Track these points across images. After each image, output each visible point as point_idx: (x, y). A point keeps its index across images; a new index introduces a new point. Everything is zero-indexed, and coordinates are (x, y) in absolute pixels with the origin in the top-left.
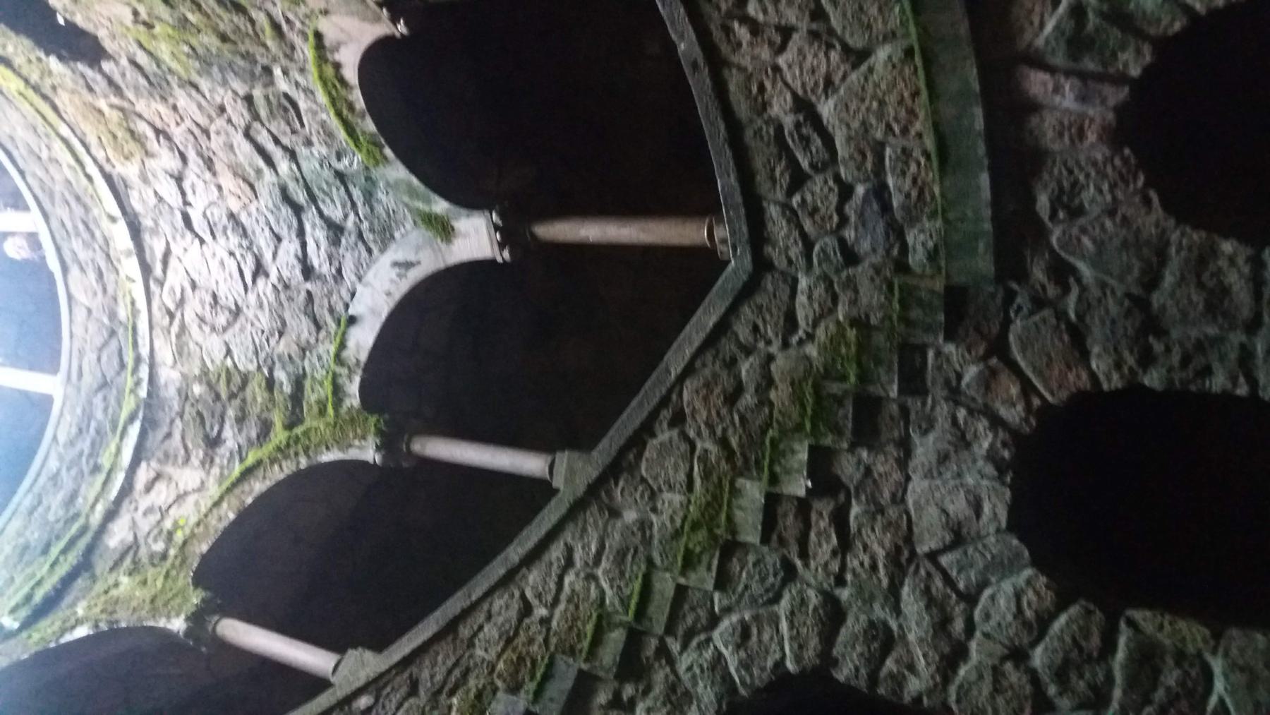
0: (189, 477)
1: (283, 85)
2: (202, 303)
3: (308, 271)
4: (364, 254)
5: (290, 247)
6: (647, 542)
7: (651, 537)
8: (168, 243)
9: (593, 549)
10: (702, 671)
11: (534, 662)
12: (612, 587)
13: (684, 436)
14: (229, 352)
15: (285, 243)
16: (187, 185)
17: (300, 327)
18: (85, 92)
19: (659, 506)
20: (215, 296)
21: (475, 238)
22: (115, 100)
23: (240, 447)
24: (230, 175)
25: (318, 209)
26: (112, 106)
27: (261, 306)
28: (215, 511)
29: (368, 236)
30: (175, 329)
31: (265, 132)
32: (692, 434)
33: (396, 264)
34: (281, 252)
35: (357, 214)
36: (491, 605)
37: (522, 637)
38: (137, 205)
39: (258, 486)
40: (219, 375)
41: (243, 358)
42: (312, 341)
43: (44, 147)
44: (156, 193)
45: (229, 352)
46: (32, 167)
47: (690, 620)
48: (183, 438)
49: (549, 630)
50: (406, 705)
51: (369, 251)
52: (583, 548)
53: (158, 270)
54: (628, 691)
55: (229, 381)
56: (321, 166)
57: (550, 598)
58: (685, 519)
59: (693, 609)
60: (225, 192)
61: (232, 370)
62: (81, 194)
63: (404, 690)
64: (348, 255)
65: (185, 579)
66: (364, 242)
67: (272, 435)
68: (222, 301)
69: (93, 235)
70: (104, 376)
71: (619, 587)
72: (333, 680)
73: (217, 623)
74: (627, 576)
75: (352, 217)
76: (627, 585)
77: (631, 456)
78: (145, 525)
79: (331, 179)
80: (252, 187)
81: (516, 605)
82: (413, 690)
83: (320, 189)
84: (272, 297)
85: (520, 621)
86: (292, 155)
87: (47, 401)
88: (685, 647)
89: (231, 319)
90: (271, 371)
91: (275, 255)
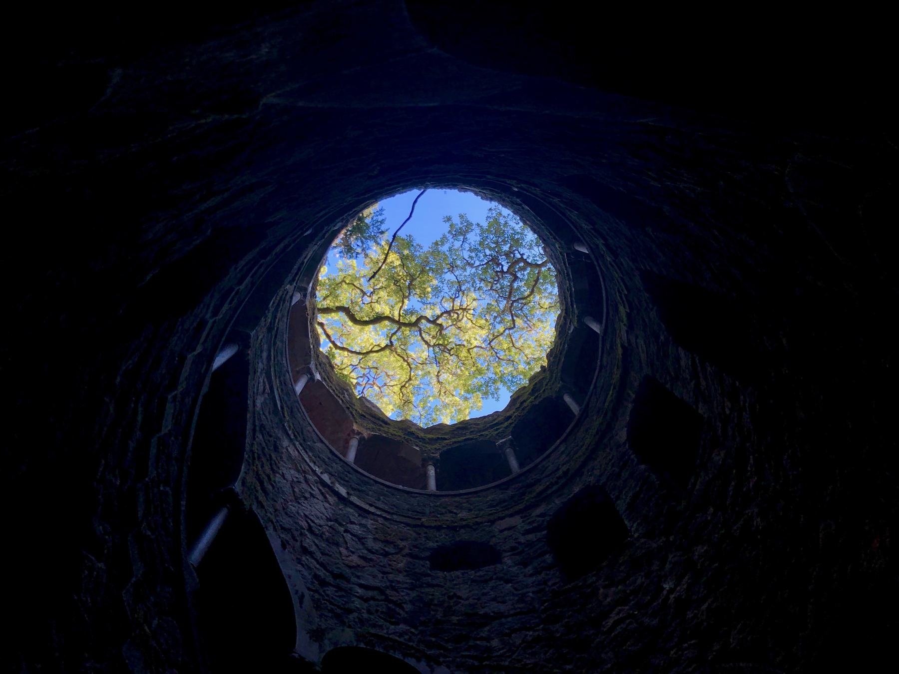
22: (407, 551)
86: (366, 600)
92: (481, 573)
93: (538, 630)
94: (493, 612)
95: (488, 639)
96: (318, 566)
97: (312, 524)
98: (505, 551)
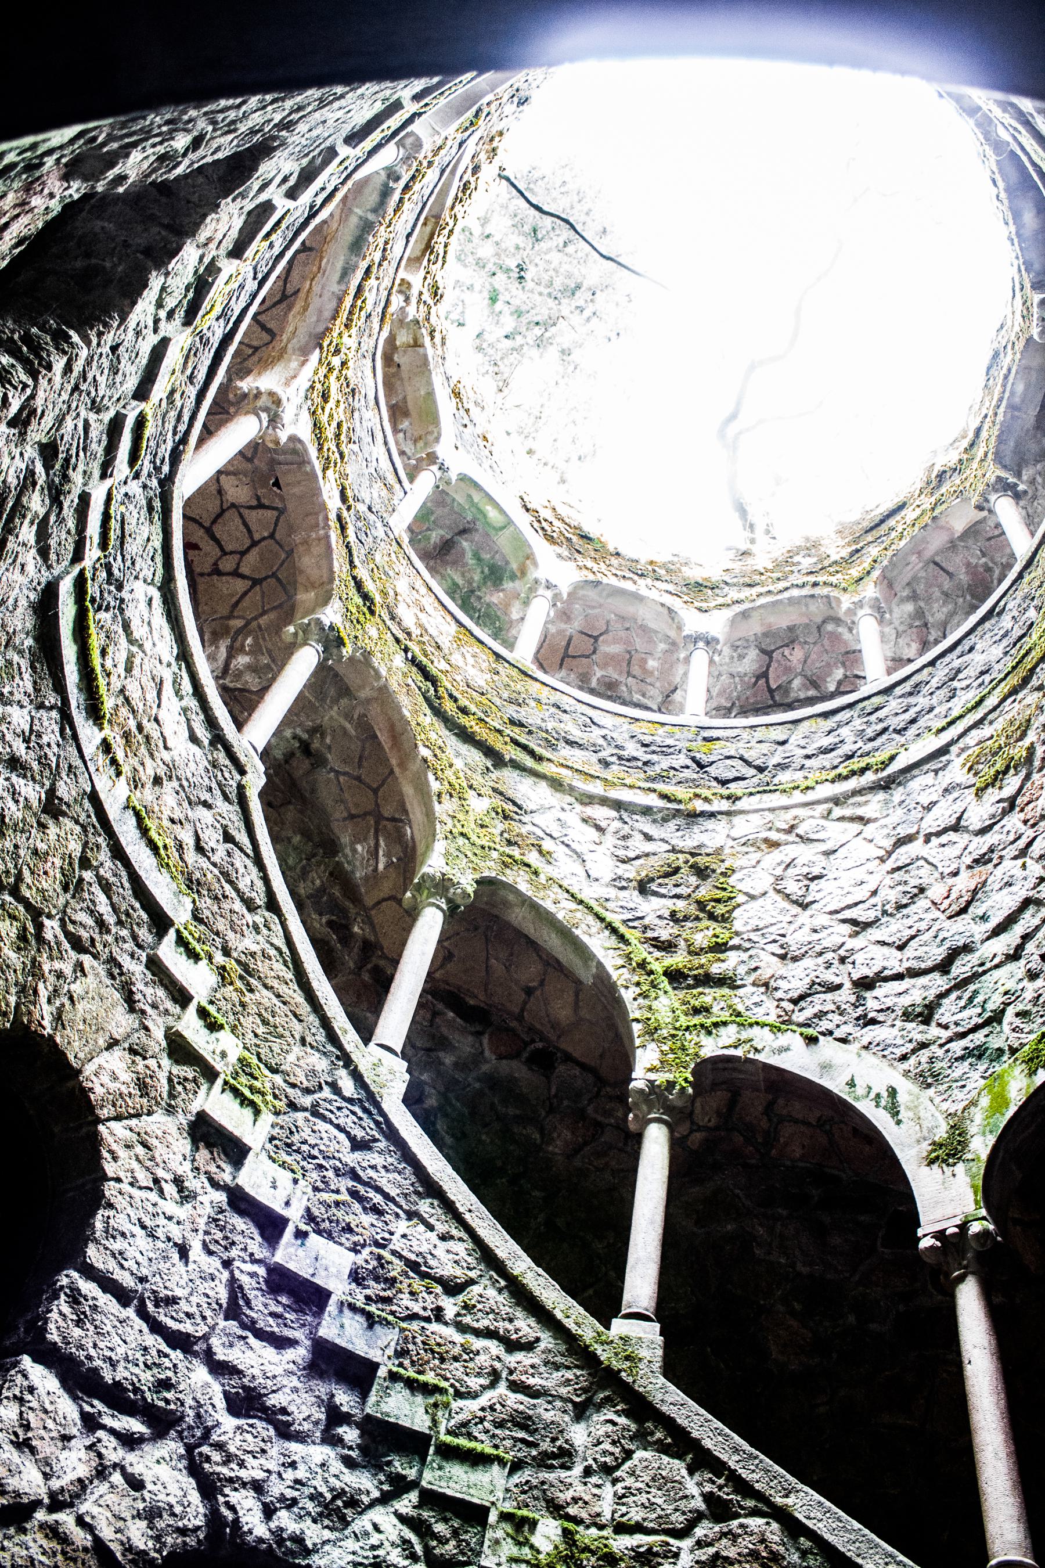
2: (811, 864)
3: (865, 984)
4: (899, 1052)
5: (895, 962)
6: (543, 1462)
7: (551, 1467)
8: (876, 820)
9: (531, 1381)
10: (373, 1548)
11: (387, 1300)
12: (483, 1409)
13: (697, 1518)
14: (752, 897)
15: (898, 954)
16: (952, 836)
17: (796, 978)
19: (594, 1480)
21: (947, 1200)
23: (642, 918)
25: (948, 992)
28: (566, 895)
29: (924, 1055)
30: (774, 836)
32: (699, 1532)
33: (893, 1092)
34: (885, 950)
35: (950, 1040)
36: (460, 1239)
37: (418, 1284)
38: (915, 785)
39: (599, 944)
40: (725, 889)
41: (749, 915)
42: (779, 994)
43: (968, 682)
44: (935, 803)
45: (752, 897)
46: (941, 672)
47: (440, 1528)
49: (427, 1320)
50: (342, 1137)
51: (904, 1058)
52: (533, 1366)
53: (838, 812)
54: (350, 1434)
55: (718, 901)
57: (467, 1320)
58: (577, 1521)
59: (455, 1533)
61: (733, 902)
62: (922, 723)
63: (359, 1133)
64: (895, 1031)
65: (490, 869)
66: (914, 1051)
67: (658, 954)
68: (813, 886)
69: (871, 740)
71: (482, 1420)
72: (372, 1044)
73: (438, 907)
74: (498, 1432)
75: (945, 1034)
76: (487, 1432)
77: (659, 1435)
78: (546, 821)
79: (990, 1006)
80: (964, 911)
81: (459, 1274)
82: (358, 1145)
83: (976, 992)
84: (826, 943)
85: (440, 1280)
86: (1015, 956)
88: (403, 1519)
89: (794, 898)
90: (737, 948)
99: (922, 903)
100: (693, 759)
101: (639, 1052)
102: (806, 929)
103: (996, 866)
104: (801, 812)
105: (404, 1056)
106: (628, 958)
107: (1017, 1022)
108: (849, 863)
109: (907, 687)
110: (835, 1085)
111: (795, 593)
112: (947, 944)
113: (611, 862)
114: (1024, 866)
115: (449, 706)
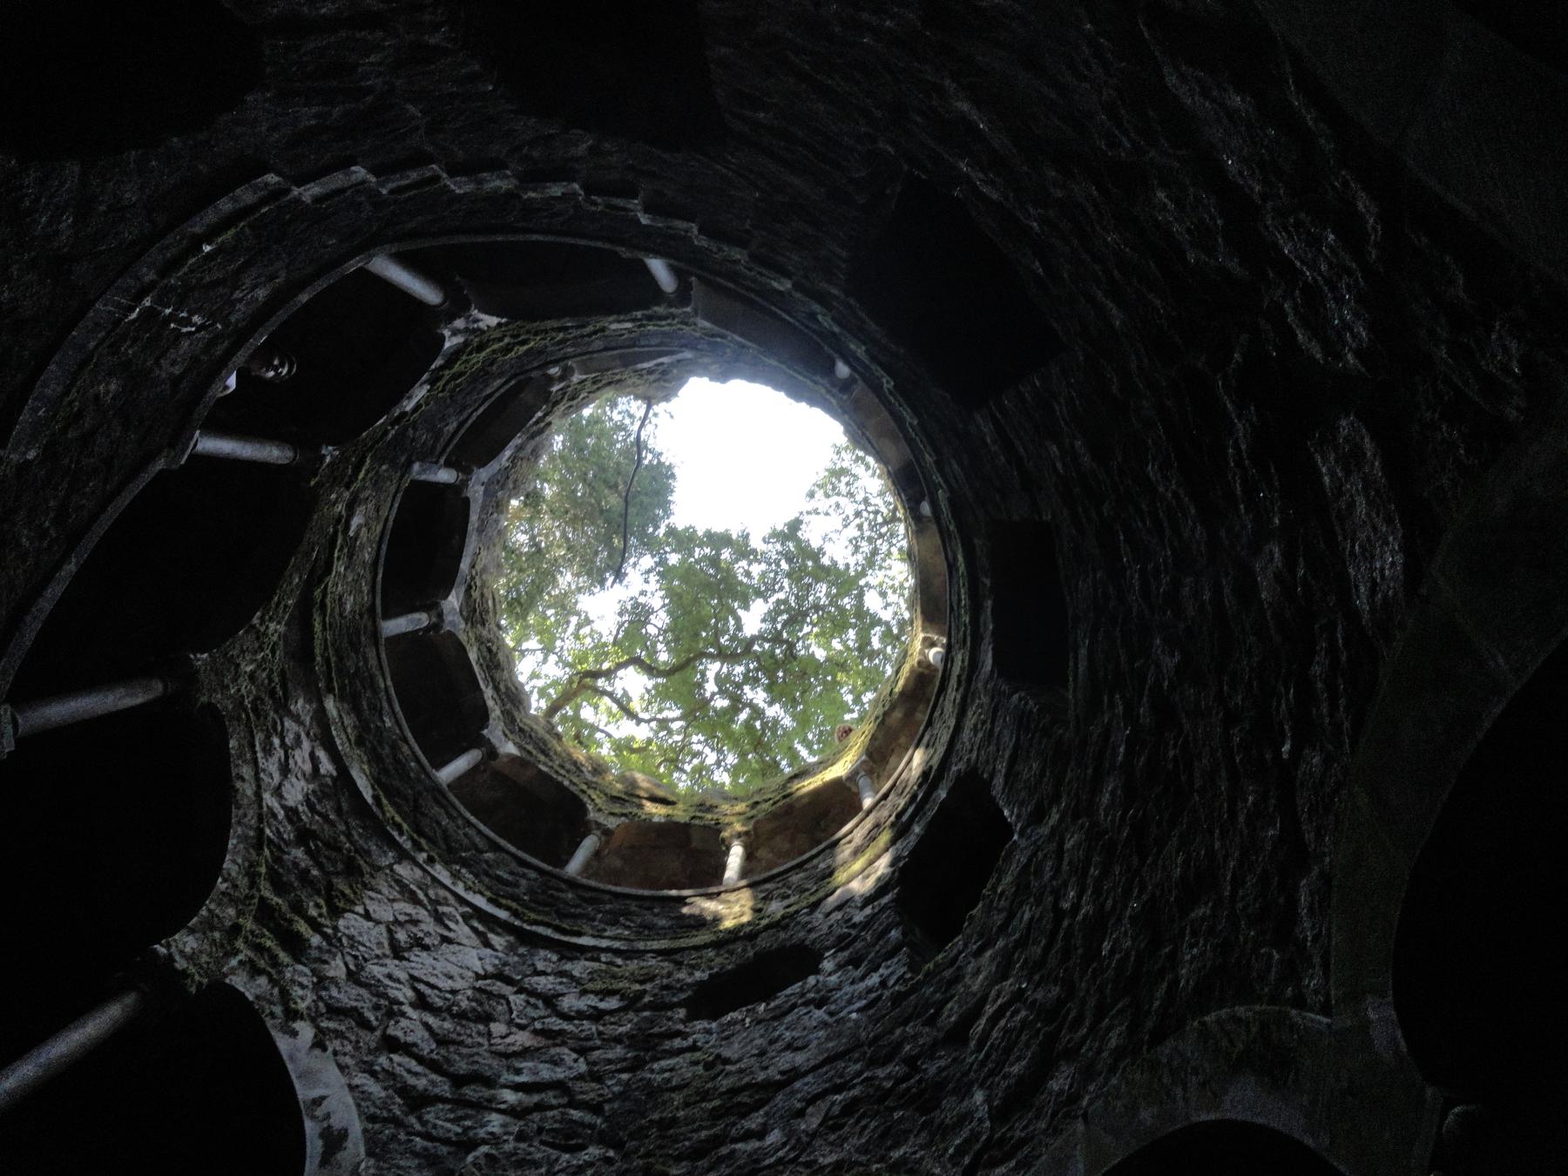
0: (295, 792)
1: (594, 1151)
3: (392, 1045)
5: (427, 1047)
14: (367, 916)
16: (540, 1003)
17: (348, 996)
18: (665, 981)
20: (426, 948)
22: (647, 999)
24: (528, 1044)
25: (444, 1100)
26: (645, 991)
27: (390, 976)
30: (421, 895)
31: (554, 1102)
33: (344, 1134)
34: (426, 1035)
42: (324, 993)
45: (367, 916)
46: (616, 906)
48: (325, 817)
56: (492, 1133)
60: (514, 1029)
66: (385, 1120)
70: (423, 814)
83: (466, 1117)
84: (393, 993)
87: (440, 765)
91: (427, 1026)
92: (777, 1002)
93: (854, 1086)
94: (782, 1073)
95: (761, 1134)
96: (419, 1069)
97: (428, 991)
98: (828, 949)
99: (481, 1027)
100: (416, 801)
101: (184, 931)
102: (386, 971)
103: (556, 1045)
104: (452, 900)
105: (20, 742)
106: (251, 865)
107: (482, 1162)
108: (453, 959)
109: (588, 895)
110: (304, 1093)
111: (566, 783)
112: (476, 1067)
113: (300, 797)
114: (576, 1061)
115: (317, 593)
